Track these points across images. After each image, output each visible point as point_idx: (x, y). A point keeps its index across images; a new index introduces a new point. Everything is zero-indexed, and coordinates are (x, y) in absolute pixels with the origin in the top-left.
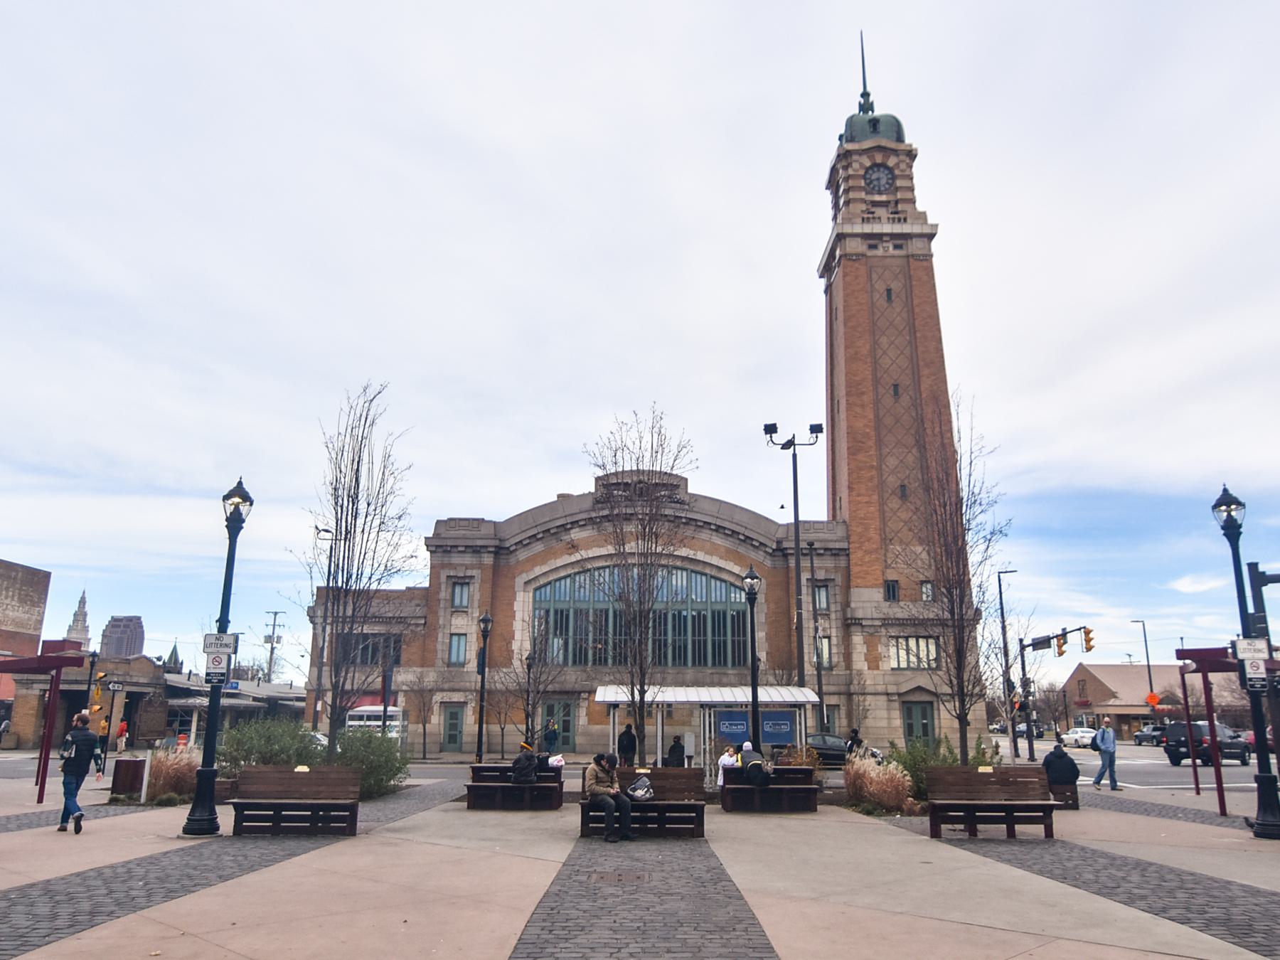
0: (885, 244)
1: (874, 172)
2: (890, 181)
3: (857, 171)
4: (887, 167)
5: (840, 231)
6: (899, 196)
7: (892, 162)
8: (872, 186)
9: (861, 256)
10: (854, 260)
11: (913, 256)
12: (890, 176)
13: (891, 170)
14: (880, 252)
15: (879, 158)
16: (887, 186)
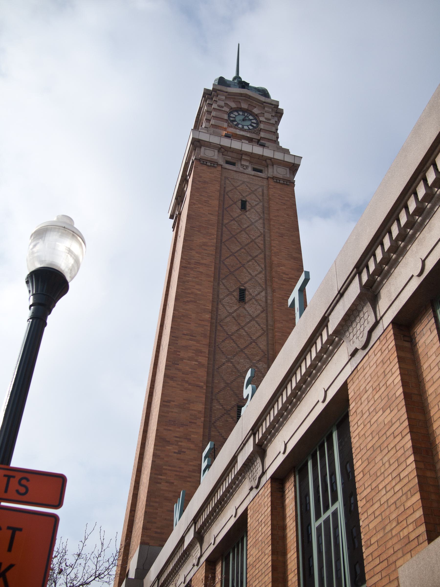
0: (244, 163)
1: (239, 114)
2: (255, 125)
3: (222, 107)
4: (252, 114)
5: (197, 137)
6: (262, 134)
7: (256, 111)
8: (235, 123)
9: (214, 164)
10: (208, 166)
11: (273, 178)
12: (254, 121)
13: (256, 116)
14: (239, 167)
15: (244, 106)
16: (251, 127)
